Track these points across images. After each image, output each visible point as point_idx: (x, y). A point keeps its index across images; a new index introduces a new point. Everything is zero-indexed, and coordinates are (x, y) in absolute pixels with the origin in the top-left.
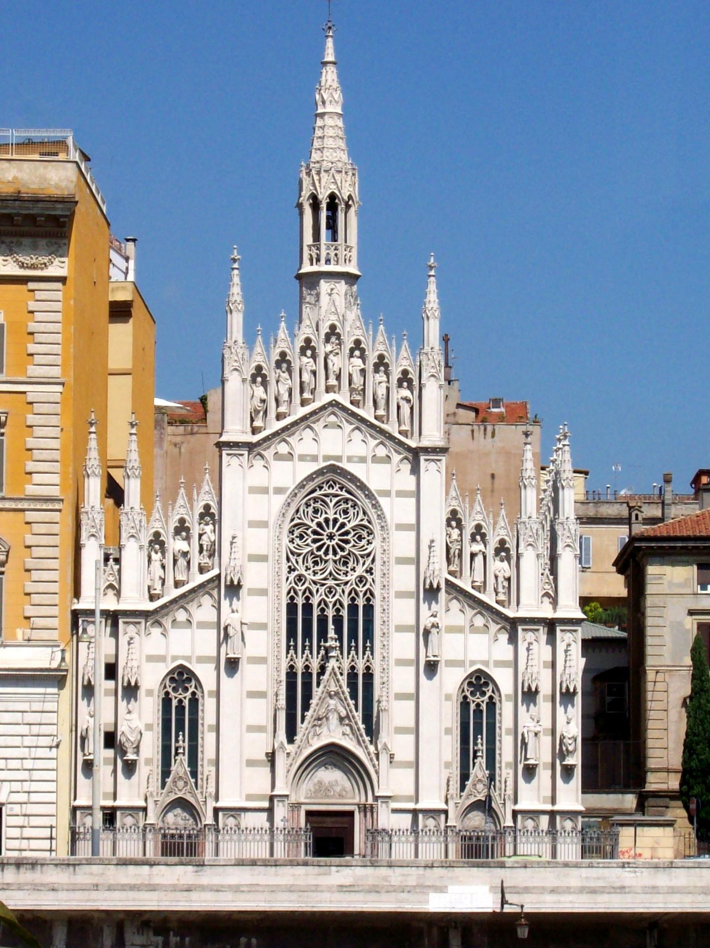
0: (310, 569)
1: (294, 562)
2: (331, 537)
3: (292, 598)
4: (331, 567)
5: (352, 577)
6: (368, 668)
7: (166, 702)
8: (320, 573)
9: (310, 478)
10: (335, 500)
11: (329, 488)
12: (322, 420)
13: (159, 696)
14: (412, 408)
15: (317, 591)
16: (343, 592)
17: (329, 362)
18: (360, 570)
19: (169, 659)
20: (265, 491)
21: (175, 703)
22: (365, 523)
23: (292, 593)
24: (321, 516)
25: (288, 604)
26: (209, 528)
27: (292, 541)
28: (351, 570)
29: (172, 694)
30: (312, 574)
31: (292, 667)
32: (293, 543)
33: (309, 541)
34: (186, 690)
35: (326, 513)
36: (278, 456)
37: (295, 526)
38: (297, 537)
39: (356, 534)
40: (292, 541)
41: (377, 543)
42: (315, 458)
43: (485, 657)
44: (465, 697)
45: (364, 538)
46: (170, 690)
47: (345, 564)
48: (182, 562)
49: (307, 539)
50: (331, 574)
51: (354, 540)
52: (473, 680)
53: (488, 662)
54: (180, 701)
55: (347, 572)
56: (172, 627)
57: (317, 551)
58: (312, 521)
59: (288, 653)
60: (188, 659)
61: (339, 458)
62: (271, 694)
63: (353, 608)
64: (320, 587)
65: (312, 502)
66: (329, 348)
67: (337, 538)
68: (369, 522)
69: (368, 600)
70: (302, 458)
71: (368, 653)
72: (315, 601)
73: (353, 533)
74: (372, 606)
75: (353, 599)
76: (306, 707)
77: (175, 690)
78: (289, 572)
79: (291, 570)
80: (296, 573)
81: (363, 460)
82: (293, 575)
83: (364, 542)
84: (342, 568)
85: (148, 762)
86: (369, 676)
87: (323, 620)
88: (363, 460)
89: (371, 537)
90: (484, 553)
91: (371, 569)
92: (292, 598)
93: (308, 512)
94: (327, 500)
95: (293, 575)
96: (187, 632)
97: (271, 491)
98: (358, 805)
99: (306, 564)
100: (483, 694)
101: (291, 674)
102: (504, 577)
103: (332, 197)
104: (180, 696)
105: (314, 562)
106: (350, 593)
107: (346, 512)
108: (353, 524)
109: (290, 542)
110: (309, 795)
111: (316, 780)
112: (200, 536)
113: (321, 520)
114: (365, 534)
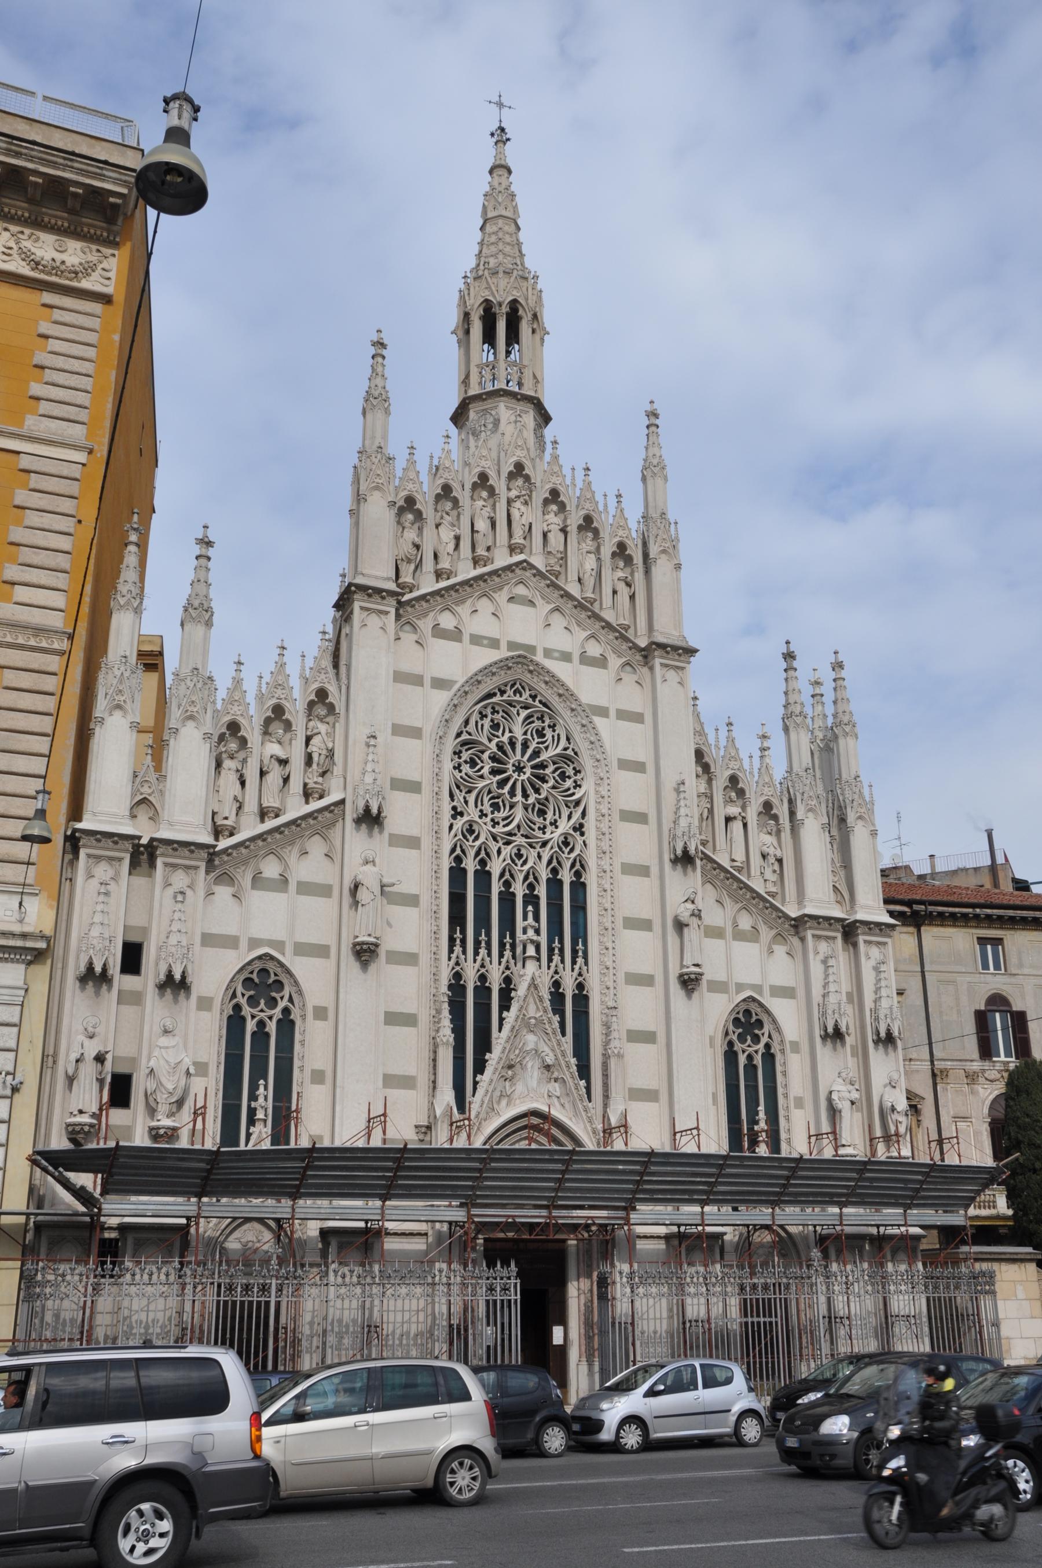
0: (486, 815)
1: (462, 800)
2: (519, 769)
3: (458, 860)
4: (519, 814)
5: (555, 836)
6: (580, 986)
7: (235, 1022)
8: (502, 823)
9: (488, 671)
10: (524, 713)
11: (515, 693)
12: (506, 588)
13: (222, 1011)
14: (632, 597)
15: (499, 852)
16: (539, 857)
17: (515, 514)
18: (564, 826)
19: (244, 944)
20: (417, 680)
21: (250, 1026)
22: (570, 752)
24: (503, 735)
25: (451, 869)
26: (322, 728)
27: (458, 768)
28: (551, 824)
29: (247, 1011)
30: (490, 824)
31: (458, 976)
32: (460, 771)
33: (486, 771)
34: (272, 1003)
35: (510, 731)
36: (439, 632)
37: (464, 743)
38: (466, 762)
41: (588, 786)
42: (494, 644)
43: (756, 980)
44: (731, 1044)
45: (569, 777)
46: (243, 1002)
47: (542, 813)
49: (482, 768)
50: (519, 827)
52: (741, 1016)
54: (261, 1024)
55: (545, 827)
56: (253, 887)
57: (498, 788)
58: (490, 740)
59: (451, 951)
60: (279, 945)
61: (532, 649)
63: (554, 884)
64: (503, 847)
65: (489, 710)
66: (514, 493)
67: (528, 771)
68: (576, 753)
69: (578, 874)
71: (580, 961)
72: (495, 867)
73: (551, 768)
74: (584, 885)
75: (555, 871)
76: (484, 1044)
77: (253, 1001)
79: (457, 813)
80: (466, 818)
81: (566, 657)
82: (459, 823)
83: (569, 783)
84: (536, 819)
86: (582, 999)
87: (507, 899)
88: (566, 657)
89: (579, 776)
90: (744, 818)
91: (581, 826)
92: (458, 860)
93: (482, 725)
95: (459, 823)
97: (427, 682)
99: (480, 807)
101: (457, 987)
102: (775, 856)
103: (514, 305)
104: (262, 1014)
105: (492, 805)
106: (550, 862)
107: (541, 734)
108: (551, 752)
109: (455, 768)
112: (308, 740)
113: (505, 739)
114: (570, 771)
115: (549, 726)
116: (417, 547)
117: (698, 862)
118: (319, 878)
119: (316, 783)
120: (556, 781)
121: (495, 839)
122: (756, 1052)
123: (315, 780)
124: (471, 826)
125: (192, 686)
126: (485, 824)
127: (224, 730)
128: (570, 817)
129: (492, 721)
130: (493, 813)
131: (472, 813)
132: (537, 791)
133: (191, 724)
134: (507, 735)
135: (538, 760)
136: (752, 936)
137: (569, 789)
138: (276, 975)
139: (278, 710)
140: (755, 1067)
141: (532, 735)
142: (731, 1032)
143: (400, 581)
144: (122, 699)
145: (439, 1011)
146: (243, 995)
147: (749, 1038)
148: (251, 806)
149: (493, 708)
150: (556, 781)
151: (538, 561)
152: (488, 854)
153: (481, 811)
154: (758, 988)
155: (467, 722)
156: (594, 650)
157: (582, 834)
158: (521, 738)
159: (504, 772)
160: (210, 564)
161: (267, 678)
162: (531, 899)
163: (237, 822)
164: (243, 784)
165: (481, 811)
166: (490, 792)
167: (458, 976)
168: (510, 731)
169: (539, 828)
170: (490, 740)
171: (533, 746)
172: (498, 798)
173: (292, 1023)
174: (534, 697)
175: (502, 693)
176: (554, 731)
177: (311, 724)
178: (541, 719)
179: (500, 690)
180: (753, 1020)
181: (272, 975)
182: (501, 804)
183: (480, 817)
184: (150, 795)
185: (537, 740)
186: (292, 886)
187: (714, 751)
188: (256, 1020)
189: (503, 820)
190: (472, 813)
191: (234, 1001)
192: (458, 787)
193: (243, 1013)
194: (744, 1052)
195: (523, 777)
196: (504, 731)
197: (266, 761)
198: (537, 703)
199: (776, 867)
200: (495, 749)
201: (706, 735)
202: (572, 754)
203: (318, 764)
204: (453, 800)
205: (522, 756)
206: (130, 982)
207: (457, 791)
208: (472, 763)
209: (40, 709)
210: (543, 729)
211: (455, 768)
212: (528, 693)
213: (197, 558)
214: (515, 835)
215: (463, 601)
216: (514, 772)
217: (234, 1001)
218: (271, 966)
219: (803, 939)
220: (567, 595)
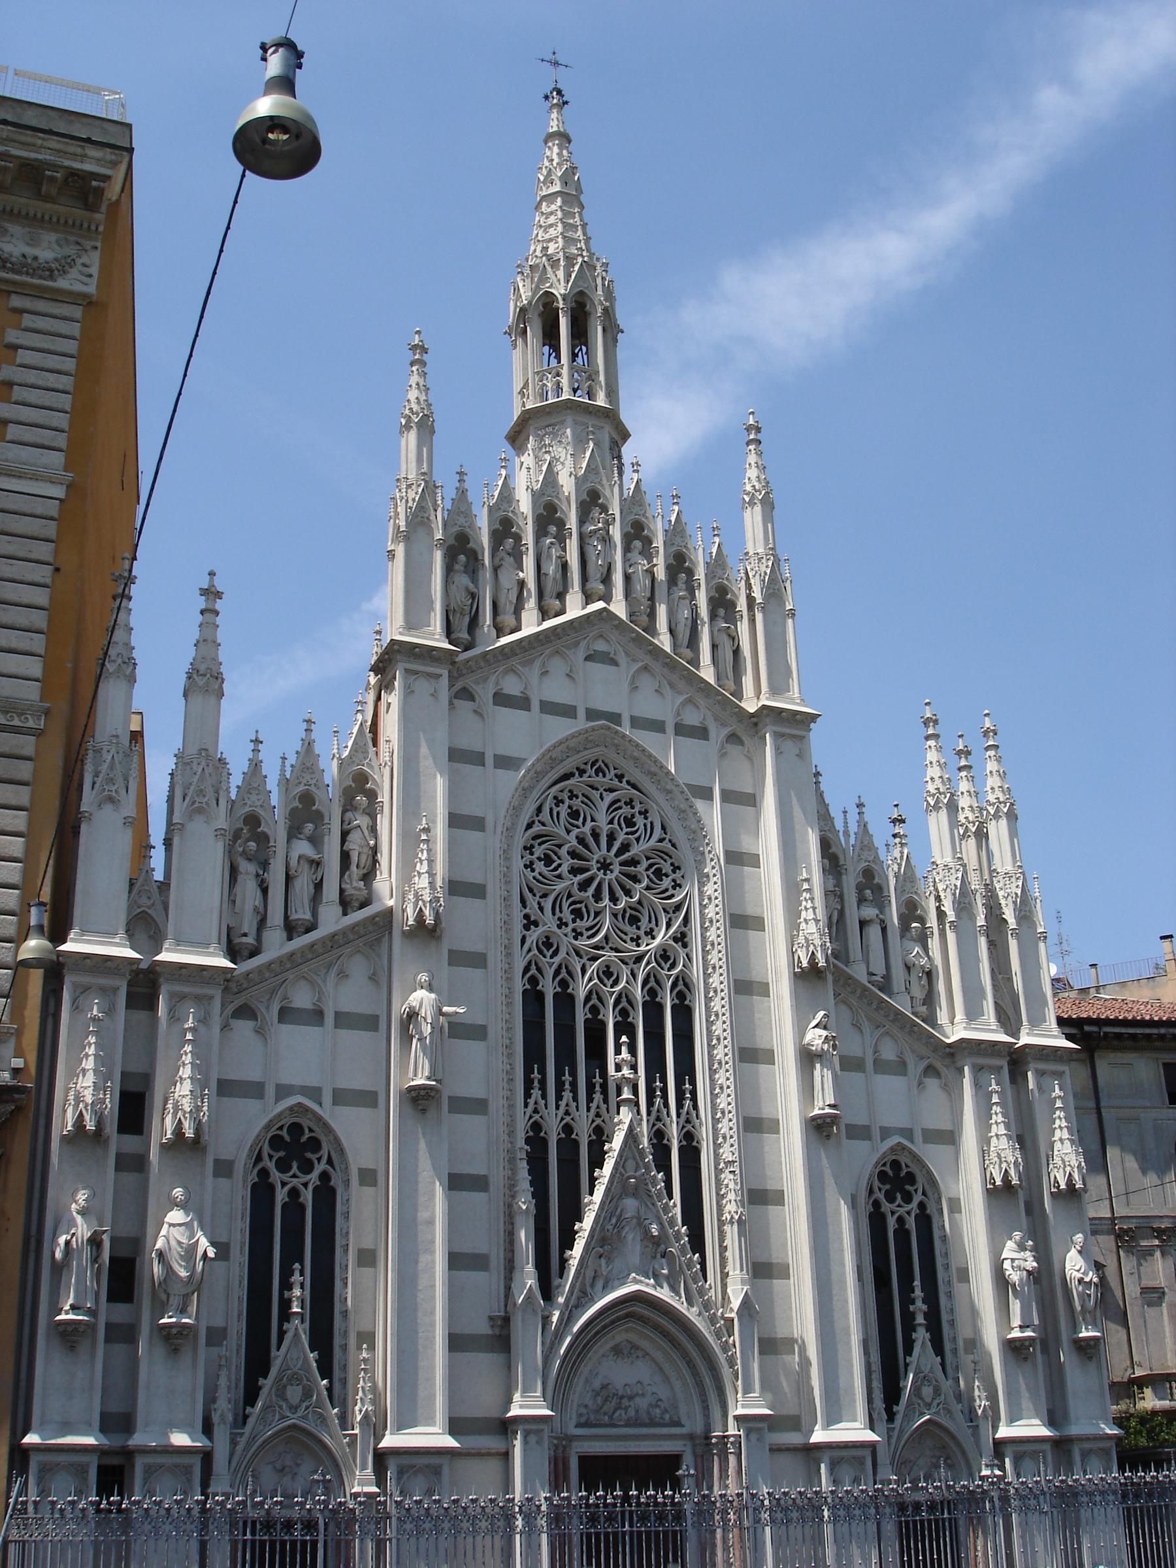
0: (566, 925)
1: (536, 907)
2: (605, 866)
3: (533, 981)
7: (262, 1192)
10: (609, 797)
12: (583, 644)
16: (634, 975)
19: (270, 1091)
20: (478, 759)
21: (281, 1196)
22: (666, 845)
23: (533, 971)
25: (525, 992)
26: (362, 821)
27: (530, 866)
29: (276, 1176)
31: (536, 1127)
32: (533, 870)
33: (564, 869)
34: (307, 1167)
35: (593, 820)
36: (501, 699)
38: (539, 859)
39: (651, 866)
40: (530, 866)
42: (568, 711)
44: (876, 1204)
45: (667, 875)
46: (271, 1165)
47: (634, 920)
48: (303, 885)
49: (560, 865)
50: (606, 938)
51: (648, 877)
52: (887, 1169)
53: (911, 1130)
54: (294, 1193)
55: (639, 938)
57: (580, 890)
58: (568, 832)
59: (527, 1095)
60: (315, 1093)
61: (615, 718)
62: (497, 1181)
63: (653, 1010)
65: (565, 796)
67: (617, 868)
68: (674, 845)
70: (549, 708)
72: (581, 989)
73: (645, 864)
75: (652, 993)
76: (573, 1212)
77: (283, 1166)
78: (527, 927)
79: (530, 923)
80: (541, 929)
82: (534, 935)
83: (666, 883)
84: (627, 928)
85: (216, 1336)
88: (658, 726)
89: (678, 874)
91: (684, 935)
92: (533, 981)
93: (558, 813)
94: (596, 795)
95: (534, 935)
96: (311, 1032)
97: (489, 760)
98: (691, 1437)
100: (908, 1198)
101: (536, 1140)
104: (295, 1180)
105: (572, 912)
106: (646, 982)
107: (630, 822)
109: (526, 866)
110: (583, 1420)
111: (597, 1384)
113: (587, 829)
114: (667, 868)
115: (640, 813)
116: (473, 596)
117: (830, 978)
118: (362, 1007)
119: (355, 888)
120: (651, 880)
121: (578, 954)
122: (908, 1213)
123: (355, 884)
124: (547, 938)
125: (200, 770)
126: (566, 935)
127: (240, 825)
128: (669, 925)
129: (570, 807)
130: (574, 921)
131: (549, 923)
132: (628, 893)
133: (199, 820)
134: (589, 824)
135: (627, 855)
136: (899, 1068)
137: (667, 890)
138: (311, 1130)
139: (307, 799)
140: (907, 1233)
141: (619, 824)
142: (876, 1189)
143: (453, 636)
144: (114, 788)
145: (514, 1171)
146: (271, 1157)
147: (899, 1196)
148: (276, 916)
149: (570, 791)
150: (651, 880)
151: (619, 608)
152: (569, 973)
153: (560, 919)
154: (908, 1133)
155: (539, 810)
156: (692, 718)
157: (685, 946)
158: (605, 829)
159: (588, 870)
160: (219, 620)
161: (292, 759)
162: (625, 1027)
163: (259, 938)
164: (265, 891)
165: (560, 919)
166: (570, 896)
167: (536, 1127)
168: (593, 820)
169: (632, 940)
170: (568, 832)
171: (621, 837)
172: (580, 902)
173: (332, 1192)
174: (620, 777)
175: (582, 772)
176: (646, 818)
177: (349, 815)
178: (630, 803)
179: (578, 769)
180: (903, 1174)
181: (307, 1131)
182: (584, 910)
183: (559, 927)
184: (149, 908)
185: (625, 830)
186: (329, 1019)
187: (842, 839)
188: (287, 1188)
189: (588, 929)
190: (549, 923)
191: (259, 1166)
192: (531, 890)
193: (271, 1180)
194: (893, 1213)
195: (610, 876)
196: (585, 820)
197: (294, 863)
198: (624, 784)
199: (924, 982)
200: (575, 842)
201: (831, 819)
202: (669, 846)
203: (358, 867)
204: (525, 907)
205: (608, 851)
206: (131, 1143)
207: (530, 895)
208: (548, 861)
209: (14, 802)
210: (633, 816)
211: (526, 866)
212: (613, 772)
213: (202, 612)
214: (602, 948)
215: (531, 662)
216: (599, 869)
217: (259, 1166)
218: (306, 1123)
219: (961, 1071)
220: (657, 652)
